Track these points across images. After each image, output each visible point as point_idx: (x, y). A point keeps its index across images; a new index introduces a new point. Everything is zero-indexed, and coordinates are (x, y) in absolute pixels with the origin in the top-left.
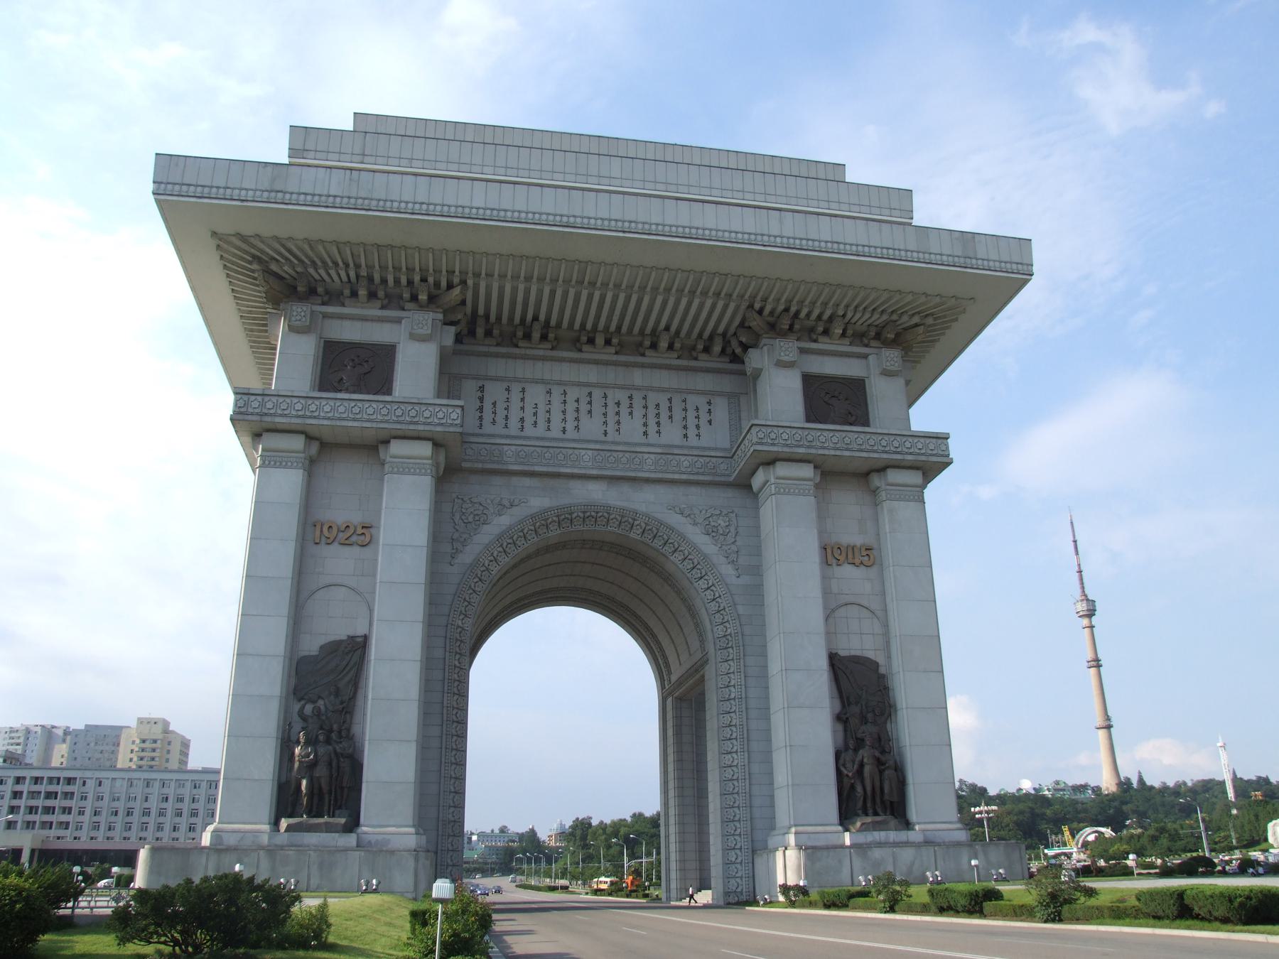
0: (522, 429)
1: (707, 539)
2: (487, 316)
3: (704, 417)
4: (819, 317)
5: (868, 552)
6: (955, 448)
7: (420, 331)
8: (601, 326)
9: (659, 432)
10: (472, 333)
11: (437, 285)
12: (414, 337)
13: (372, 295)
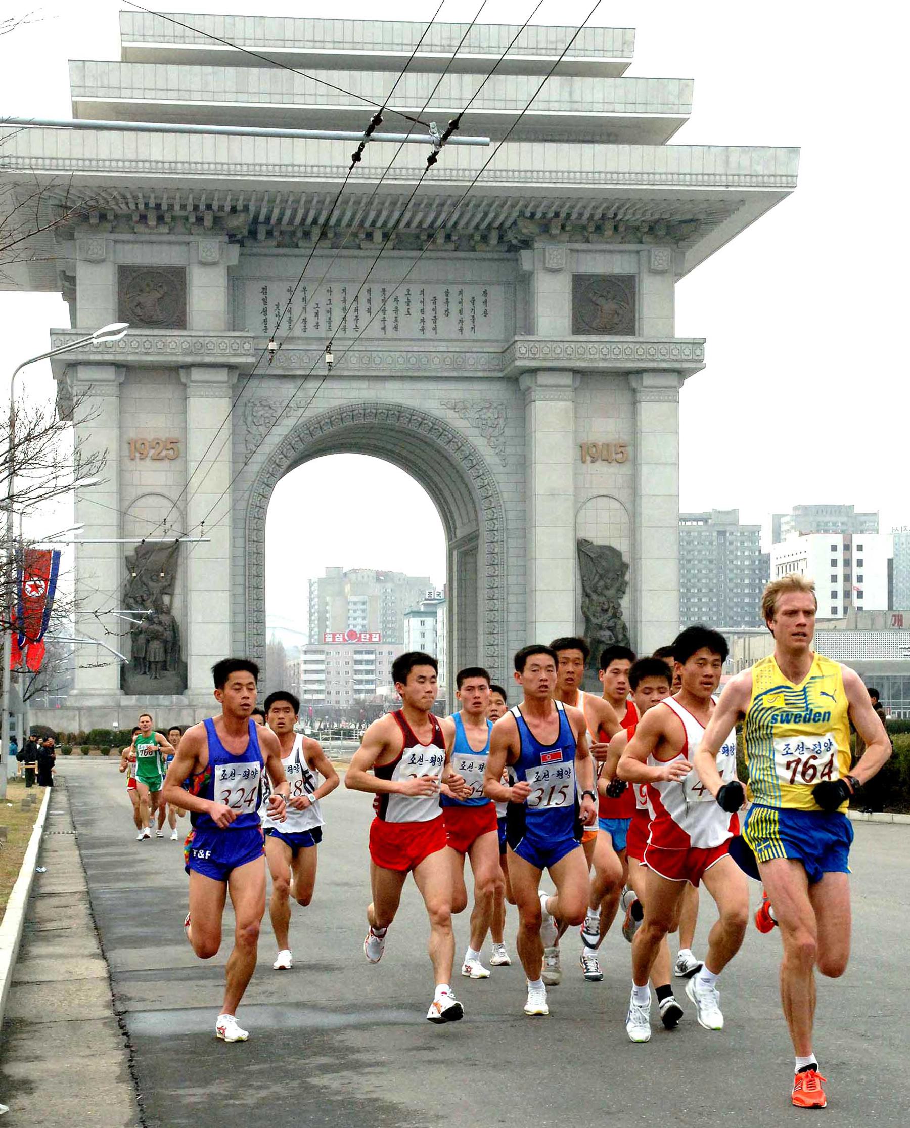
0: (305, 330)
1: (476, 432)
2: (268, 219)
3: (480, 309)
4: (592, 216)
5: (622, 449)
6: (710, 354)
7: (210, 259)
8: (379, 223)
9: (435, 329)
10: (253, 234)
11: (221, 208)
12: (204, 264)
13: (160, 219)
